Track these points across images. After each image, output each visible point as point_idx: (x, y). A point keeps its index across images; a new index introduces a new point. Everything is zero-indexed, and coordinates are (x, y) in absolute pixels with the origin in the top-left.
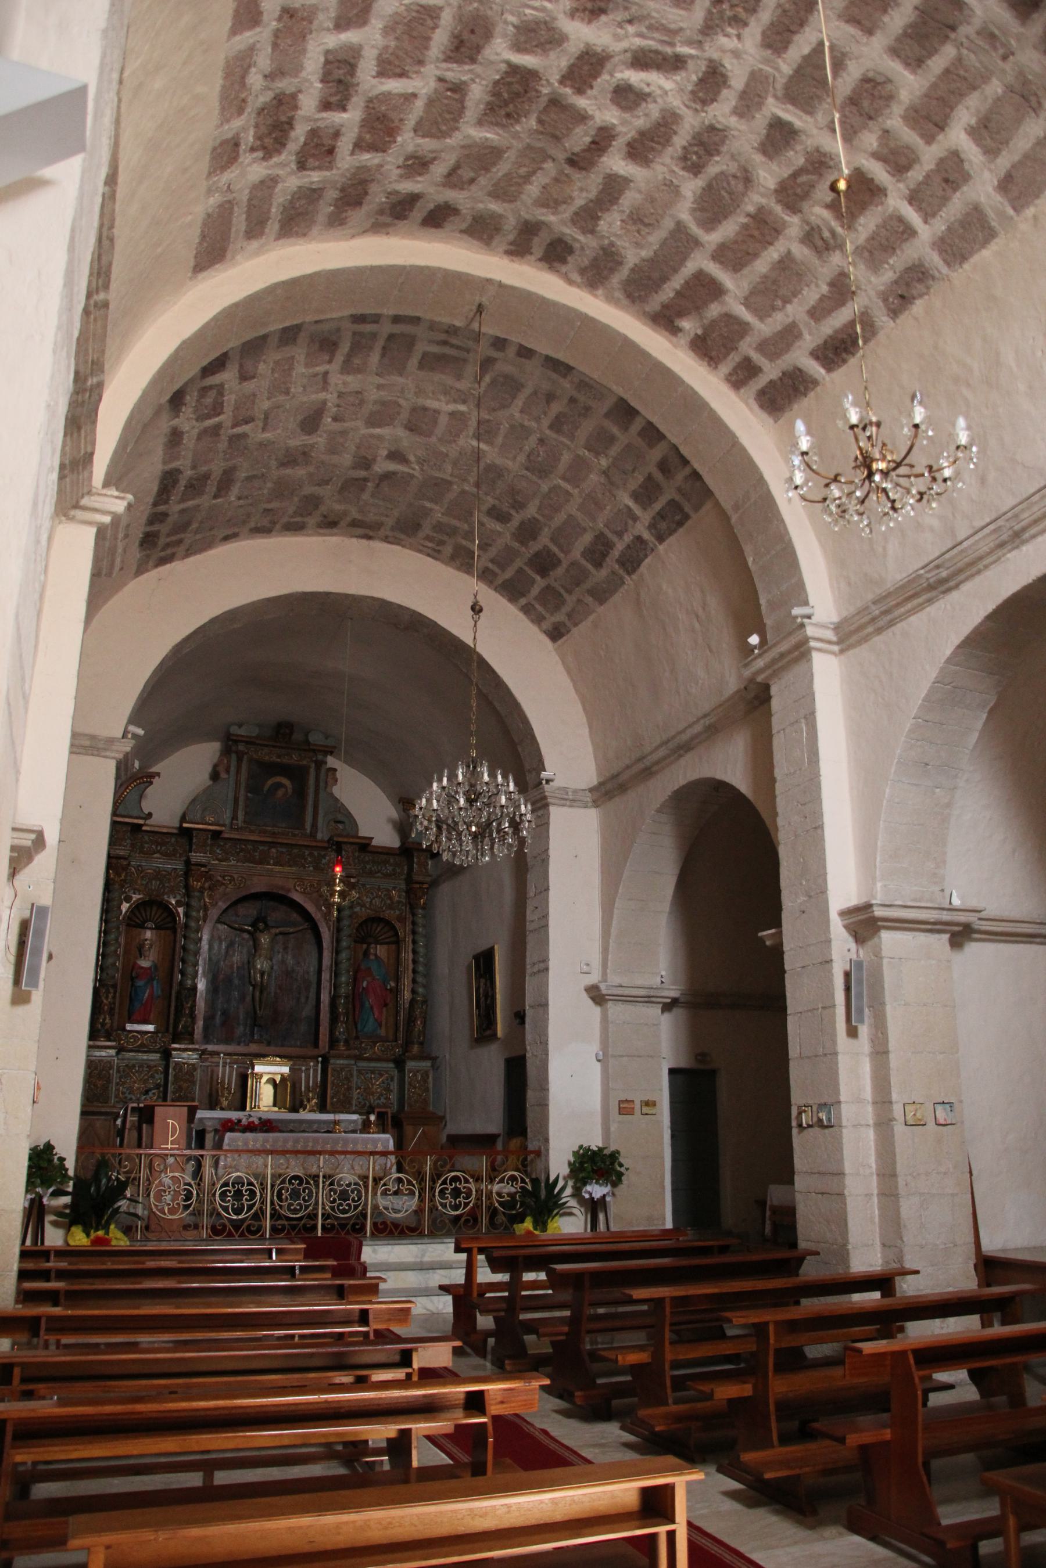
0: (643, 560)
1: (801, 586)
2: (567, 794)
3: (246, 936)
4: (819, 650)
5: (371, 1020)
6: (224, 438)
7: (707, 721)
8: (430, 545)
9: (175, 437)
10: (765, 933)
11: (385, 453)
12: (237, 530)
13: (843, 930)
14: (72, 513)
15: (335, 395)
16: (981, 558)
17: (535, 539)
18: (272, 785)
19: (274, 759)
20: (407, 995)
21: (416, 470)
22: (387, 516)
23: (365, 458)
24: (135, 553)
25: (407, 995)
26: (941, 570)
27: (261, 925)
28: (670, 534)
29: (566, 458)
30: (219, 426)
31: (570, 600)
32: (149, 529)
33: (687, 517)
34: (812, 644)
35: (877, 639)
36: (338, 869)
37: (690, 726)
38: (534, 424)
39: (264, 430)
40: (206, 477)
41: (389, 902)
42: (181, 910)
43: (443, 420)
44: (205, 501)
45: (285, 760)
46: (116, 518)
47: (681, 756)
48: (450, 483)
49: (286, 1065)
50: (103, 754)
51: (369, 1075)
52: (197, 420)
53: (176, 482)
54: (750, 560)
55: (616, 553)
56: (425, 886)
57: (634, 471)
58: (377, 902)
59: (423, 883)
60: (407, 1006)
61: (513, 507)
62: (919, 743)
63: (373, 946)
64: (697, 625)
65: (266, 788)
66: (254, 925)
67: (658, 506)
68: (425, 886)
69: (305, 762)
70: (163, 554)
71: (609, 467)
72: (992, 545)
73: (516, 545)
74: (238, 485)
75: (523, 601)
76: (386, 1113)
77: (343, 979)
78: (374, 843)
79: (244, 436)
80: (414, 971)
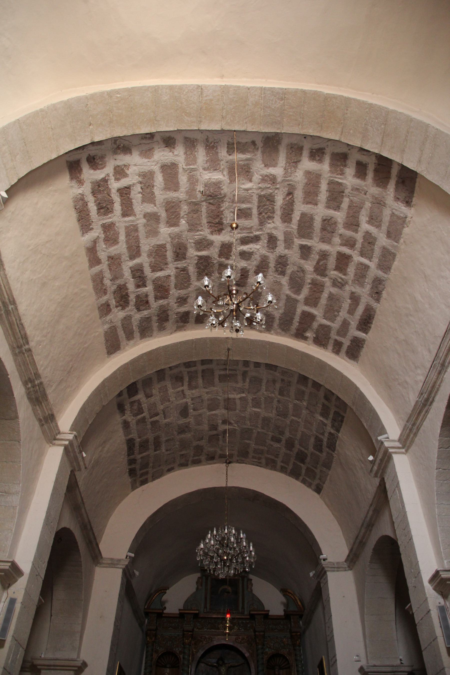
0: (336, 443)
1: (383, 427)
2: (334, 564)
3: (215, 669)
4: (396, 453)
6: (148, 423)
7: (372, 508)
8: (256, 460)
9: (126, 425)
10: (407, 607)
11: (221, 421)
12: (172, 466)
13: (434, 591)
14: (54, 442)
15: (190, 399)
16: (435, 383)
17: (293, 447)
21: (236, 427)
22: (233, 450)
23: (214, 425)
24: (127, 479)
26: (424, 395)
27: (221, 662)
28: (341, 427)
29: (291, 406)
30: (144, 418)
31: (318, 471)
32: (130, 467)
33: (343, 417)
34: (390, 450)
35: (416, 439)
36: (228, 616)
37: (368, 513)
38: (273, 395)
39: (165, 418)
40: (147, 441)
41: (282, 645)
42: (181, 656)
43: (238, 402)
44: (151, 452)
46: (71, 442)
47: (371, 531)
48: (252, 430)
50: (116, 566)
52: (133, 416)
53: (134, 445)
54: (365, 424)
55: (325, 443)
56: (299, 634)
57: (317, 404)
61: (280, 434)
62: (445, 482)
63: (276, 670)
64: (363, 465)
66: (217, 663)
67: (331, 416)
68: (299, 634)
70: (141, 479)
71: (307, 405)
72: (436, 374)
73: (288, 452)
74: (164, 444)
75: (301, 478)
79: (157, 421)
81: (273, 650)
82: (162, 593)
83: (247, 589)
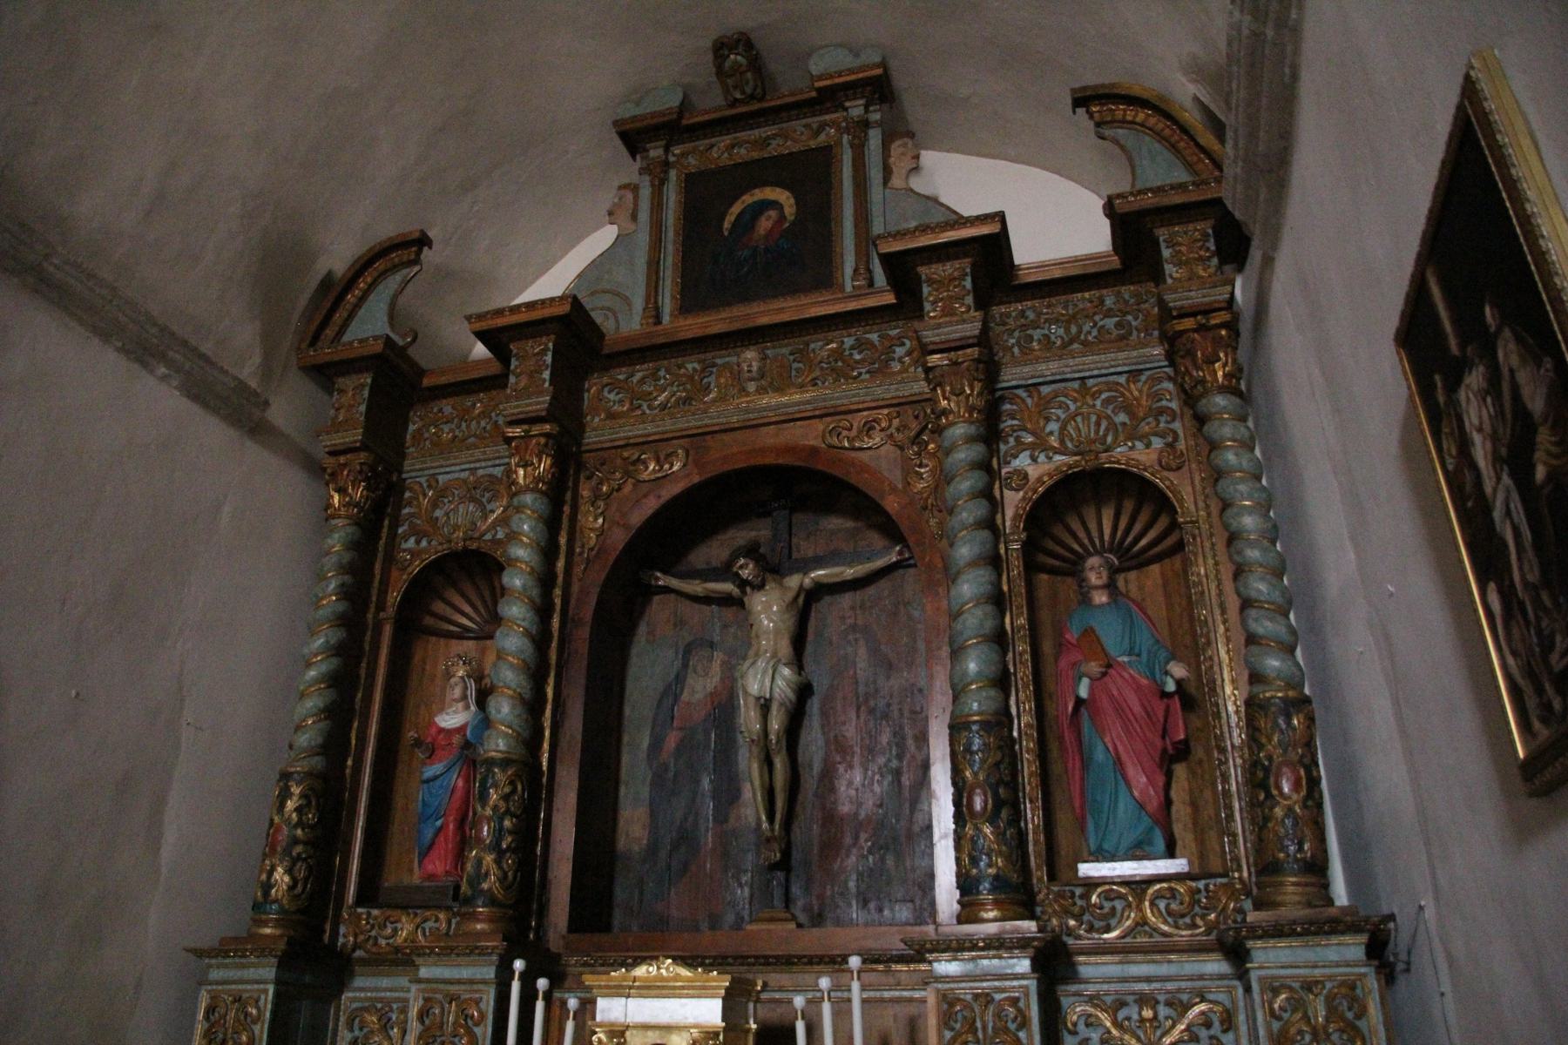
5: (1124, 807)
18: (740, 215)
19: (742, 154)
20: (1231, 698)
25: (1231, 698)
41: (1122, 418)
45: (776, 148)
49: (702, 992)
58: (1084, 429)
59: (1207, 311)
60: (1237, 737)
65: (727, 225)
80: (1246, 604)
81: (1058, 458)
82: (395, 268)
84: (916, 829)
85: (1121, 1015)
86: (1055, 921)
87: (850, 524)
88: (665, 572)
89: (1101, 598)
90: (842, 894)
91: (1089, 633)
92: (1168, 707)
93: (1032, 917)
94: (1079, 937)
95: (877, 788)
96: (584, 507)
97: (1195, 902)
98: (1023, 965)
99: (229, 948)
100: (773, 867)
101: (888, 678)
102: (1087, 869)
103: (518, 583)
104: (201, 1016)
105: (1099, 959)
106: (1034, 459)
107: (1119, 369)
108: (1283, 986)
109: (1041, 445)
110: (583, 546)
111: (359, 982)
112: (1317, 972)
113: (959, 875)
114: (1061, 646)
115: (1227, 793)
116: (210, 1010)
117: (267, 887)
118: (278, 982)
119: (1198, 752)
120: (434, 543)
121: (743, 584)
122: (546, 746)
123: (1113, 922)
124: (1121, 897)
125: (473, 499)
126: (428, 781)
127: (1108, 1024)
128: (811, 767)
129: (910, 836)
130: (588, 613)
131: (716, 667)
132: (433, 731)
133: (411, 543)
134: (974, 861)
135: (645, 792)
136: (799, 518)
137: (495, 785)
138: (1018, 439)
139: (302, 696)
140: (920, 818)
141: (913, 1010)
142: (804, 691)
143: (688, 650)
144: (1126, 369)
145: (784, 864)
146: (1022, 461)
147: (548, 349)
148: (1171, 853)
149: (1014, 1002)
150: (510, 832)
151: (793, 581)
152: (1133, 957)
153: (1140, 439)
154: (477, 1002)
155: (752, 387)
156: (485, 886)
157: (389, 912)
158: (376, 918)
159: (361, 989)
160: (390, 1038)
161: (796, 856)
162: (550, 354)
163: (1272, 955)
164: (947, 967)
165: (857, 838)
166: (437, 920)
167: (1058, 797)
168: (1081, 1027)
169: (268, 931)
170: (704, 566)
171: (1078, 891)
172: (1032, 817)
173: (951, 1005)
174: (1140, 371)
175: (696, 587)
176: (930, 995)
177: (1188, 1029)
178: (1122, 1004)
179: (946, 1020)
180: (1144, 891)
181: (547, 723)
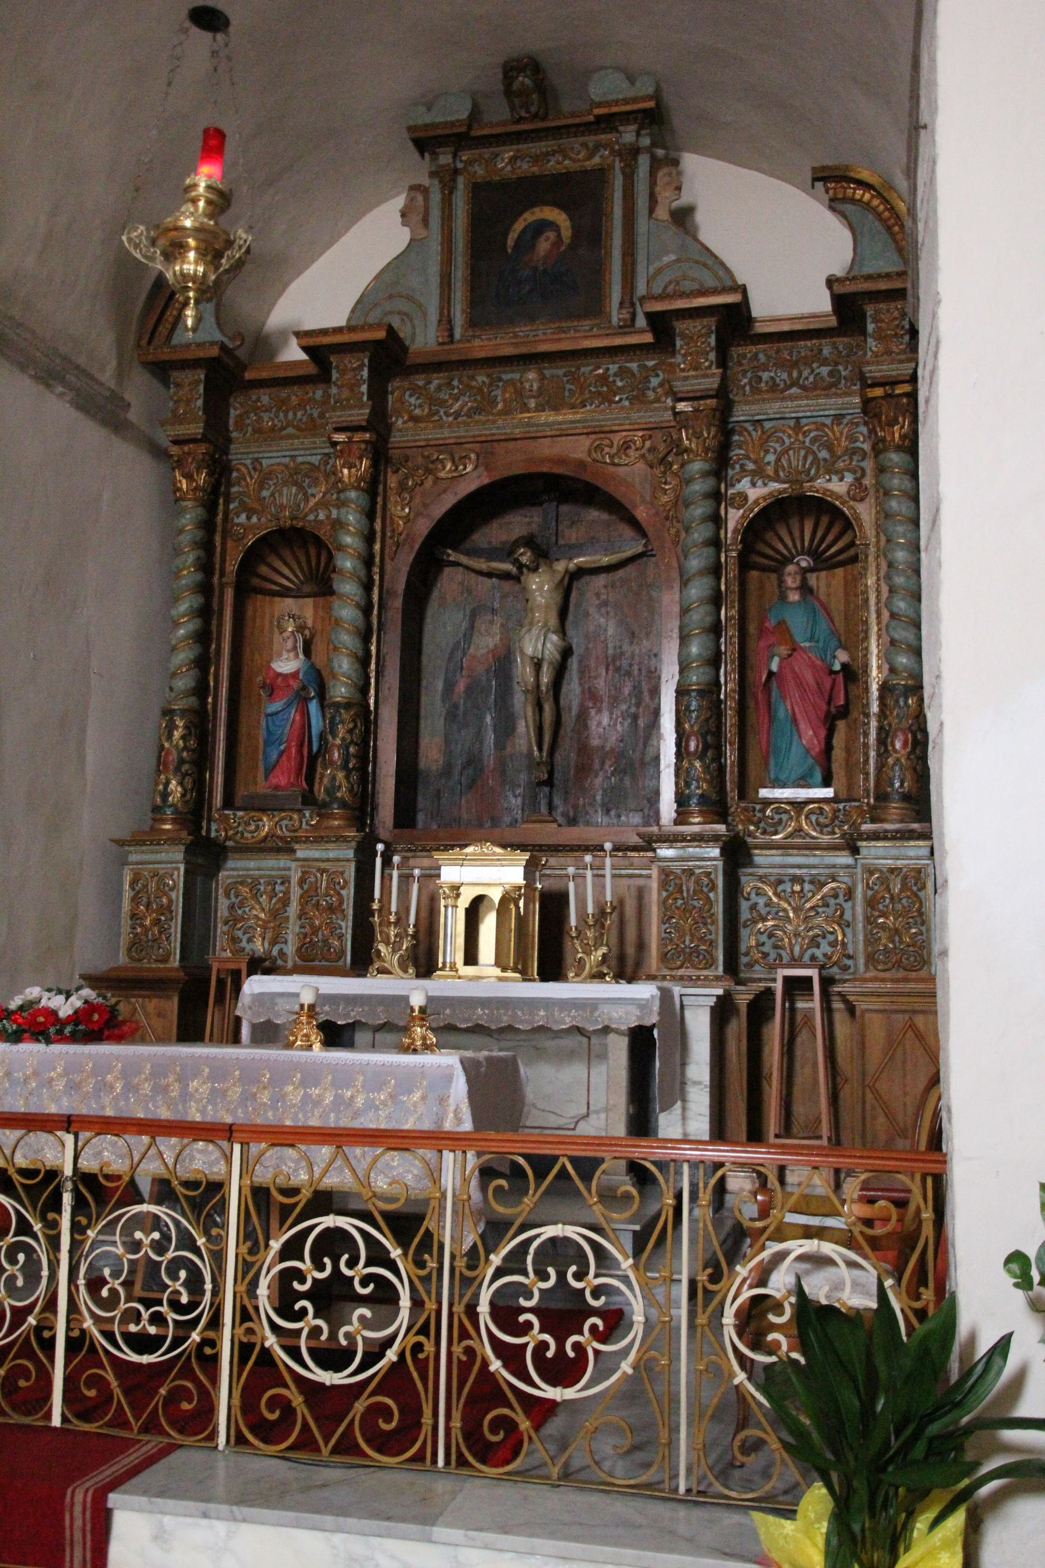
18: (524, 231)
19: (526, 168)
41: (824, 454)
45: (554, 165)
51: (787, 887)
58: (795, 460)
59: (894, 383)
65: (510, 242)
69: (597, 160)
76: (809, 980)
77: (694, 650)
78: (758, 310)
81: (775, 486)
83: (651, 211)
84: (647, 759)
85: (780, 888)
86: (740, 827)
87: (605, 516)
88: (454, 549)
89: (794, 597)
90: (590, 804)
91: (782, 626)
92: (834, 681)
93: (725, 822)
94: (755, 838)
95: (619, 727)
96: (393, 498)
97: (835, 817)
98: (715, 852)
99: (137, 840)
100: (540, 784)
101: (632, 643)
102: (764, 793)
103: (348, 564)
104: (127, 887)
105: (767, 852)
106: (754, 485)
107: (827, 413)
108: (877, 870)
109: (759, 474)
110: (393, 531)
111: (230, 864)
112: (899, 862)
113: (677, 793)
114: (762, 631)
115: (866, 745)
116: (133, 883)
117: (165, 795)
118: (187, 862)
119: (854, 714)
120: (263, 519)
121: (520, 566)
122: (372, 692)
123: (780, 828)
124: (786, 812)
125: (295, 483)
126: (271, 715)
127: (770, 894)
128: (570, 709)
129: (643, 764)
130: (401, 587)
131: (496, 629)
132: (271, 674)
133: (243, 518)
134: (688, 785)
135: (440, 723)
136: (564, 509)
137: (342, 722)
138: (742, 466)
139: (174, 649)
140: (650, 752)
141: (641, 882)
142: (566, 653)
143: (474, 615)
144: (832, 412)
145: (549, 782)
146: (744, 485)
147: (363, 365)
148: (827, 783)
149: (708, 874)
150: (355, 756)
151: (560, 566)
152: (791, 851)
153: (836, 472)
154: (342, 873)
155: (532, 403)
156: (339, 795)
157: (252, 814)
158: (242, 818)
159: (232, 869)
160: (260, 903)
161: (558, 776)
162: (366, 370)
163: (873, 851)
164: (666, 852)
165: (603, 764)
166: (291, 819)
167: (752, 741)
168: (753, 896)
169: (168, 827)
170: (486, 546)
171: (758, 807)
172: (731, 756)
173: (667, 875)
174: (843, 416)
175: (482, 565)
176: (654, 872)
177: (822, 898)
178: (780, 882)
179: (664, 884)
180: (802, 809)
181: (373, 675)
